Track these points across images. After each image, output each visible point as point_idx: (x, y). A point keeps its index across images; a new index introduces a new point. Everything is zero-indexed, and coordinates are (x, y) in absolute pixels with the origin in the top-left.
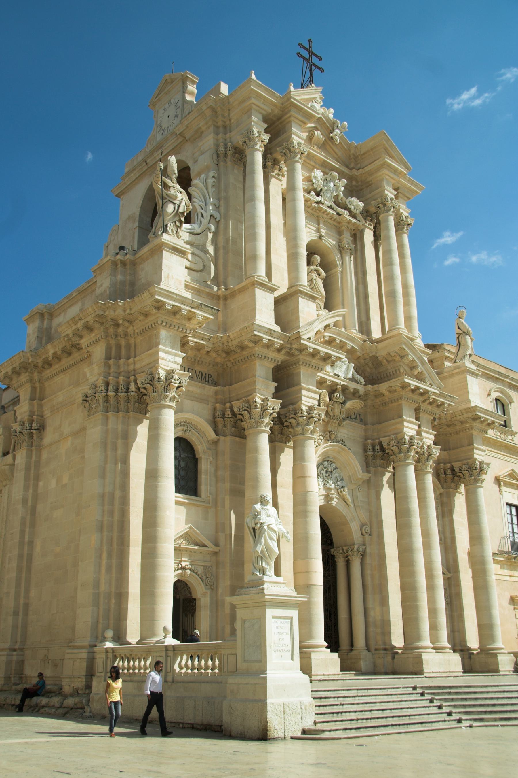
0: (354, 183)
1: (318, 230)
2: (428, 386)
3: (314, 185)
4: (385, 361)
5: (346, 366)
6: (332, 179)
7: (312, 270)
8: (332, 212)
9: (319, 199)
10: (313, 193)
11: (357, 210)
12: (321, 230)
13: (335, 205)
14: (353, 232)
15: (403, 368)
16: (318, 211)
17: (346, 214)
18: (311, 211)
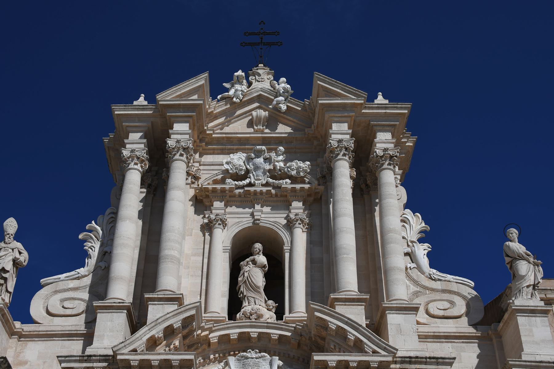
0: (315, 143)
1: (252, 215)
2: (372, 356)
3: (230, 171)
4: (319, 340)
5: (268, 361)
6: (259, 154)
7: (247, 262)
8: (265, 189)
9: (247, 181)
10: (229, 181)
11: (299, 173)
12: (255, 214)
13: (271, 180)
14: (312, 199)
15: (333, 341)
16: (249, 196)
17: (286, 183)
18: (239, 199)
